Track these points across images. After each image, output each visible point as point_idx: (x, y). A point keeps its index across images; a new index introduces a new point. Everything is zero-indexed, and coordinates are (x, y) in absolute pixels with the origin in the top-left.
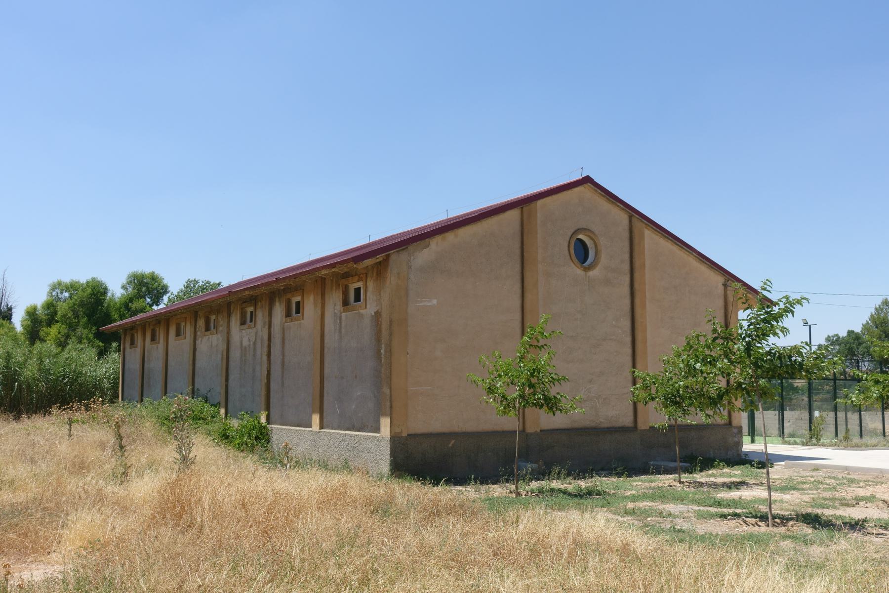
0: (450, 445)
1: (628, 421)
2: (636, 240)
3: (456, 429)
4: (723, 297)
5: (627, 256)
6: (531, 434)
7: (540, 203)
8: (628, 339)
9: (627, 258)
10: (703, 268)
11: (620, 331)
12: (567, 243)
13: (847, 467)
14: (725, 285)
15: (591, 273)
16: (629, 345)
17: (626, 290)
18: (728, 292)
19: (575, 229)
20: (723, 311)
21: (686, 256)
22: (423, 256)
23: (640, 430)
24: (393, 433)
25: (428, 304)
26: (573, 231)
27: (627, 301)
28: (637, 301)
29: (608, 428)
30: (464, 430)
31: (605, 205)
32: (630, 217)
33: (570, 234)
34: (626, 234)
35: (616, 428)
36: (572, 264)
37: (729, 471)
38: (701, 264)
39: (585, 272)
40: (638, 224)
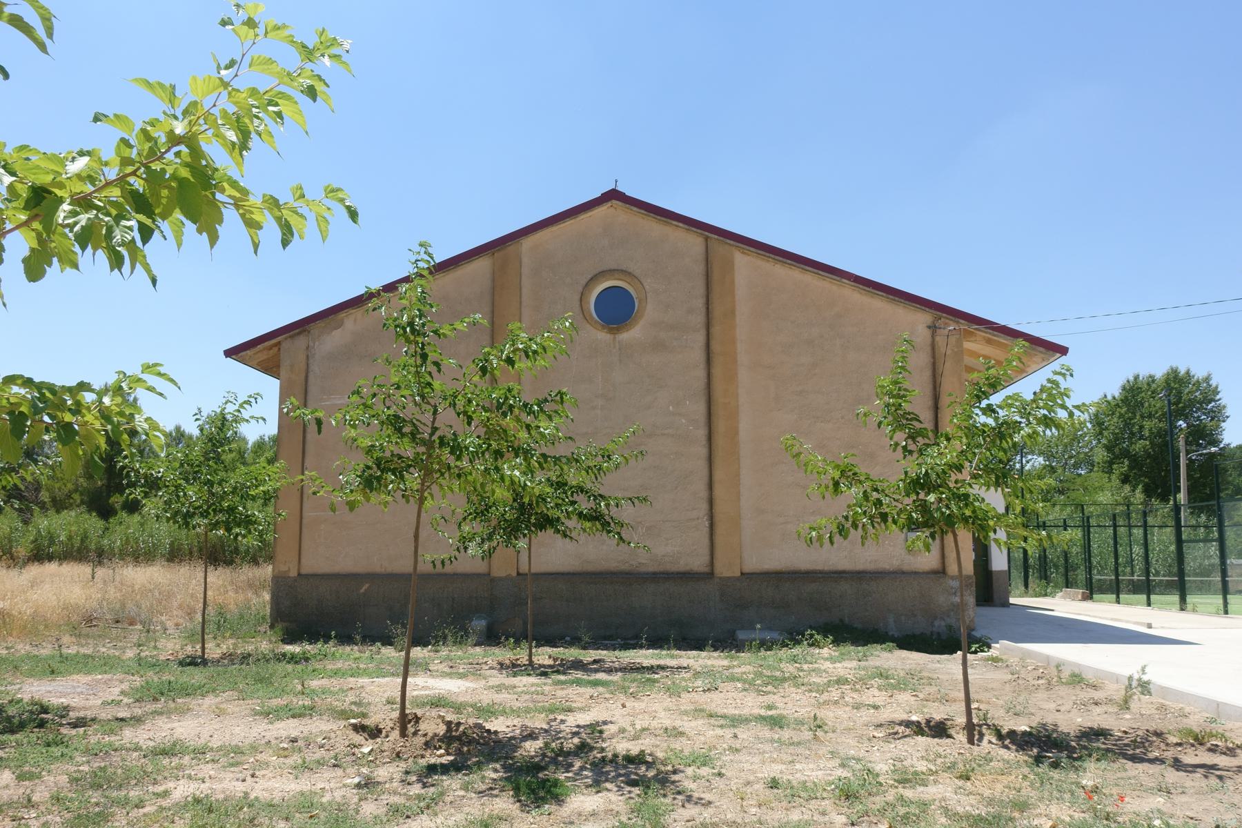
0: (362, 591)
1: (698, 562)
2: (716, 275)
3: (378, 569)
4: (929, 349)
5: (700, 303)
6: (501, 579)
7: (527, 243)
8: (702, 433)
9: (701, 305)
10: (879, 304)
11: (684, 421)
12: (578, 297)
13: (1080, 665)
14: (933, 328)
15: (625, 336)
16: (703, 441)
17: (698, 355)
18: (938, 339)
19: (595, 272)
20: (927, 374)
21: (834, 288)
22: (331, 340)
23: (720, 578)
24: (276, 571)
25: (339, 402)
26: (590, 276)
27: (701, 373)
28: (717, 371)
29: (654, 573)
30: (389, 570)
31: (654, 227)
32: (707, 239)
33: (584, 281)
34: (700, 268)
35: (672, 573)
36: (588, 326)
37: (726, 663)
38: (872, 297)
39: (612, 336)
40: (721, 248)
